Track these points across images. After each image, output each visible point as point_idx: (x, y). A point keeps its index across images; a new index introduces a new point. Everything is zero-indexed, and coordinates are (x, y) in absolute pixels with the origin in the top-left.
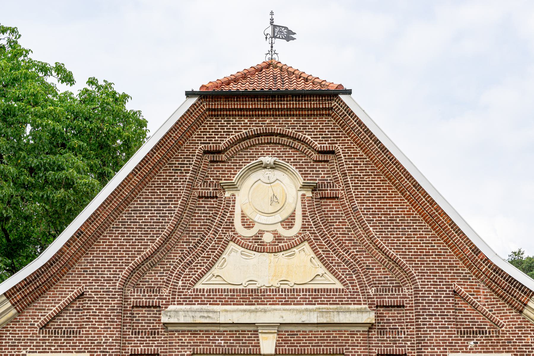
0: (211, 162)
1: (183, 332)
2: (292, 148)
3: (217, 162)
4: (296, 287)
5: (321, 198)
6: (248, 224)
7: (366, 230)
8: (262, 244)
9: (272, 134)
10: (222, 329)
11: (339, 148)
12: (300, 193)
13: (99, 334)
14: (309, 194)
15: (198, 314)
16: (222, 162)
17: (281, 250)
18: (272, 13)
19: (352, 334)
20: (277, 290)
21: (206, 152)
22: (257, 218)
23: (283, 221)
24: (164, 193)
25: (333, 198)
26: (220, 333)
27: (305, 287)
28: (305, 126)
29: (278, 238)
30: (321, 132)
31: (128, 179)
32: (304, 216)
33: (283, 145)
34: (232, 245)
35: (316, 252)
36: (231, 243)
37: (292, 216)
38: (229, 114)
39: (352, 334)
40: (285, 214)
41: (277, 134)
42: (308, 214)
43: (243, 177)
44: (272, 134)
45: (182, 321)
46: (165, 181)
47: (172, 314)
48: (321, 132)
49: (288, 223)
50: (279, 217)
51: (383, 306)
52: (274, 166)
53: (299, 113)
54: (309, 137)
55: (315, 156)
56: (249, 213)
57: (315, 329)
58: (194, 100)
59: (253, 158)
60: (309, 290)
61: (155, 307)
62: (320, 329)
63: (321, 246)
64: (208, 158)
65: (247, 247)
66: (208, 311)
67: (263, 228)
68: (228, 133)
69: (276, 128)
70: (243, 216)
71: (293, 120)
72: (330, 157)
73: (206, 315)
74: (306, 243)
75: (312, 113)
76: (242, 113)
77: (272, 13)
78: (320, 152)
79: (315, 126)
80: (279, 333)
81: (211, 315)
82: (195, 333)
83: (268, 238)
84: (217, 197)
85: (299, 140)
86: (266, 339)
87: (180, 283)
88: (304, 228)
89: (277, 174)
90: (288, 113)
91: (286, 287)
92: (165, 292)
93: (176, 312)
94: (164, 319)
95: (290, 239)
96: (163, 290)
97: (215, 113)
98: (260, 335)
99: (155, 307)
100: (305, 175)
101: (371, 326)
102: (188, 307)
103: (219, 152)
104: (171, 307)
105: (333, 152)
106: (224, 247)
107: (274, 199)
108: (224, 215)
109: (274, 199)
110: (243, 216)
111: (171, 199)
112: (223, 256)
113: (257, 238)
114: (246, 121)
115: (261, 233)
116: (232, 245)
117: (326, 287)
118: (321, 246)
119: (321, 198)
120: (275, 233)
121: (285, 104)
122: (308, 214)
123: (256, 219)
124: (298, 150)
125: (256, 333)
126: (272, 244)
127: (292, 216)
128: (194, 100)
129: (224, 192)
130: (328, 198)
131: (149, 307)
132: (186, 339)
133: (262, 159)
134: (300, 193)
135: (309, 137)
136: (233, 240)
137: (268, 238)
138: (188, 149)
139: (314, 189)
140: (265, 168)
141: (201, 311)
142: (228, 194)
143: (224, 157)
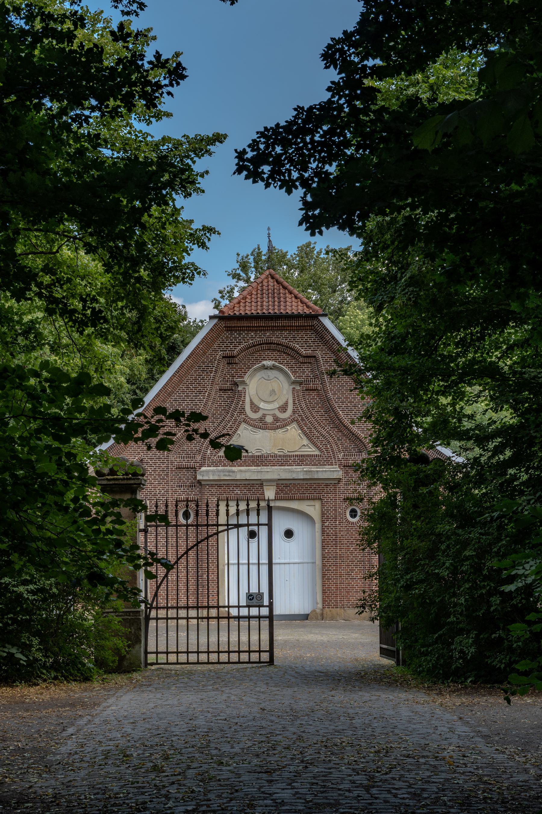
0: (228, 363)
1: (212, 486)
2: (285, 353)
3: (232, 363)
4: (288, 454)
5: (306, 390)
6: (255, 408)
7: (336, 414)
8: (265, 423)
9: (271, 343)
10: (238, 483)
11: (319, 354)
12: (292, 387)
13: (155, 488)
14: (298, 388)
15: (222, 474)
16: (235, 363)
17: (278, 428)
18: (269, 229)
19: (327, 485)
20: (276, 456)
21: (223, 357)
22: (262, 405)
23: (280, 407)
24: (195, 388)
25: (315, 390)
26: (237, 486)
27: (294, 453)
28: (294, 338)
29: (276, 419)
30: (306, 342)
31: (171, 379)
32: (294, 403)
33: (279, 351)
34: (243, 425)
35: (302, 429)
36: (243, 423)
37: (286, 404)
38: (240, 329)
39: (327, 485)
40: (281, 403)
41: (274, 344)
42: (297, 402)
43: (252, 376)
44: (271, 343)
45: (211, 478)
46: (196, 379)
47: (205, 474)
48: (306, 342)
49: (283, 408)
50: (276, 405)
51: (348, 466)
52: (273, 368)
53: (290, 328)
54: (298, 346)
55: (301, 360)
56: (256, 401)
57: (302, 482)
58: (215, 321)
59: (257, 361)
60: (297, 456)
61: (192, 468)
62: (305, 482)
63: (306, 425)
64: (225, 361)
65: (254, 426)
66: (229, 471)
67: (265, 412)
68: (240, 343)
69: (274, 339)
70: (252, 403)
71: (286, 333)
72: (312, 360)
73: (227, 474)
74: (295, 422)
75: (299, 328)
76: (249, 329)
77: (269, 229)
78: (304, 357)
79: (302, 338)
80: (278, 486)
81: (231, 474)
82: (220, 486)
83: (269, 419)
84: (232, 390)
85: (291, 348)
86: (269, 489)
87: (209, 451)
88: (294, 412)
89: (275, 373)
90: (283, 328)
91: (282, 454)
92: (199, 458)
93: (207, 472)
94: (199, 477)
95: (284, 420)
96: (197, 456)
97: (229, 329)
98: (265, 487)
99: (192, 468)
100: (295, 372)
101: (339, 480)
102: (215, 468)
103: (233, 357)
104: (203, 469)
105: (314, 357)
106: (238, 426)
107: (273, 392)
108: (237, 404)
109: (273, 392)
110: (252, 403)
111: (200, 392)
112: (239, 432)
113: (262, 419)
114: (252, 334)
115: (264, 415)
116: (243, 425)
117: (309, 453)
118: (306, 425)
119: (306, 390)
120: (274, 416)
121: (280, 323)
122: (297, 402)
123: (261, 406)
124: (289, 355)
125: (262, 485)
126: (272, 423)
127: (286, 404)
128: (215, 321)
129: (238, 386)
130: (311, 390)
131: (188, 468)
132: (214, 490)
133: (265, 362)
134: (292, 387)
135: (298, 346)
136: (245, 421)
137: (269, 419)
138: (211, 355)
139: (300, 383)
140: (267, 369)
141: (223, 471)
142: (240, 388)
143: (237, 360)
